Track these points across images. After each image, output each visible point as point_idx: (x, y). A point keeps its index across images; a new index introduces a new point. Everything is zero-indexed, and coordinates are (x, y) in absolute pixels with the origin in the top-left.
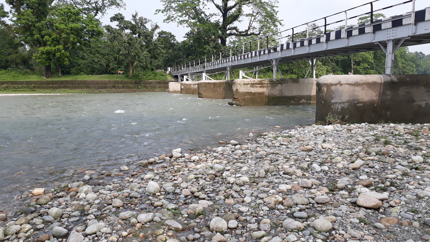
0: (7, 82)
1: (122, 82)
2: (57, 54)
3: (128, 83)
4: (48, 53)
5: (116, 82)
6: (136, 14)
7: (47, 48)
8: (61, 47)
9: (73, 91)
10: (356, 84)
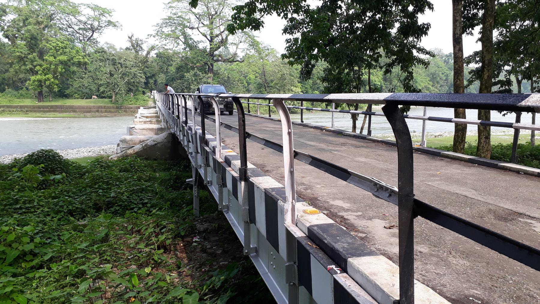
0: (3, 106)
1: (105, 107)
2: (47, 82)
3: (110, 108)
4: (40, 81)
5: (99, 107)
6: (132, 36)
7: (38, 77)
8: (50, 76)
9: (61, 115)
10: (144, 129)
